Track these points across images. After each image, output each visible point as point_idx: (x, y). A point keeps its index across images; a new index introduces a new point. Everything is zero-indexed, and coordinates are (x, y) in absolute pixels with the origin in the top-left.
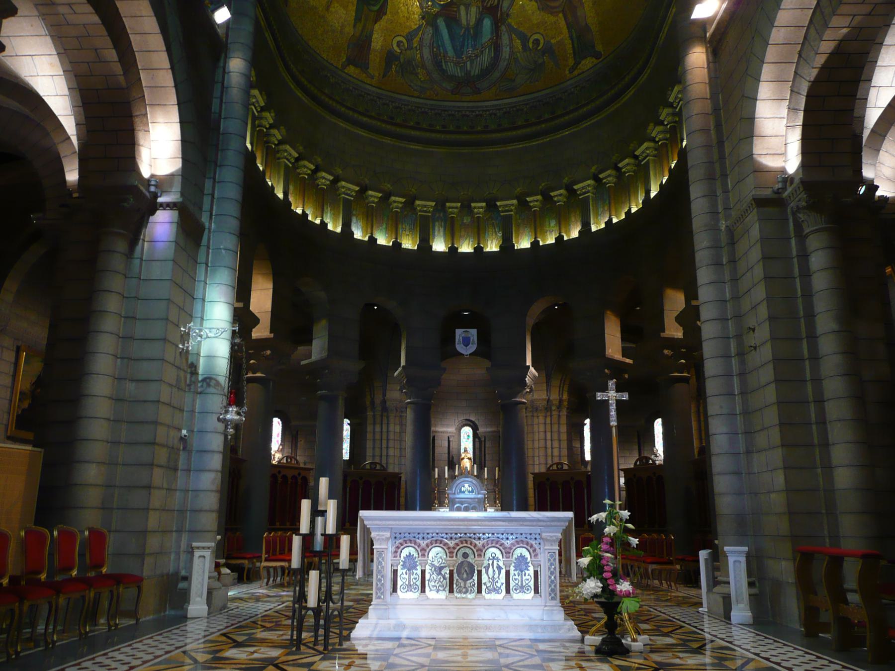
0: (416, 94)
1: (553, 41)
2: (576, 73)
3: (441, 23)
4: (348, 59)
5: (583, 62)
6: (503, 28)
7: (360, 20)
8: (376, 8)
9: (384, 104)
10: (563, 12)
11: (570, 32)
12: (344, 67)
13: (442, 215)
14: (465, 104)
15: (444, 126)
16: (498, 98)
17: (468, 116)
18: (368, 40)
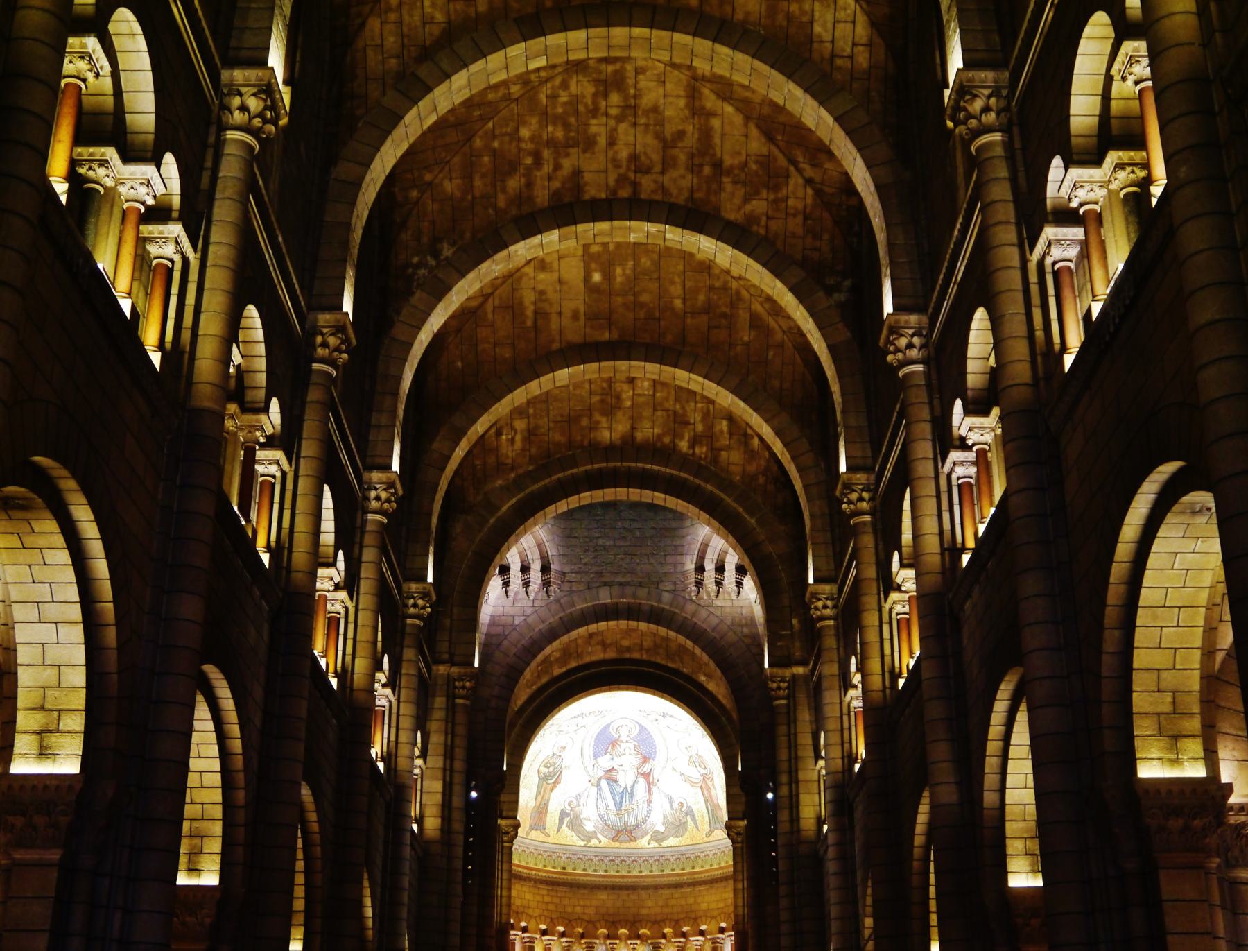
0: (582, 843)
1: (694, 808)
2: (711, 838)
3: (604, 783)
4: (531, 826)
5: (716, 831)
6: (654, 789)
7: (540, 793)
8: (552, 781)
9: (558, 857)
10: (701, 787)
11: (706, 805)
12: (528, 834)
13: (604, 948)
14: (624, 850)
15: (606, 871)
16: (650, 846)
17: (625, 861)
18: (546, 805)
